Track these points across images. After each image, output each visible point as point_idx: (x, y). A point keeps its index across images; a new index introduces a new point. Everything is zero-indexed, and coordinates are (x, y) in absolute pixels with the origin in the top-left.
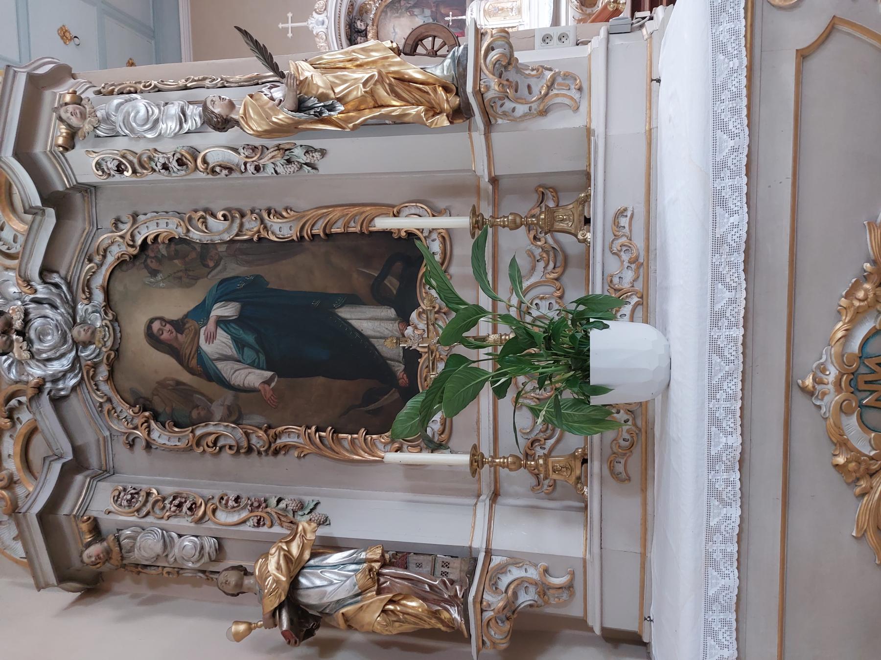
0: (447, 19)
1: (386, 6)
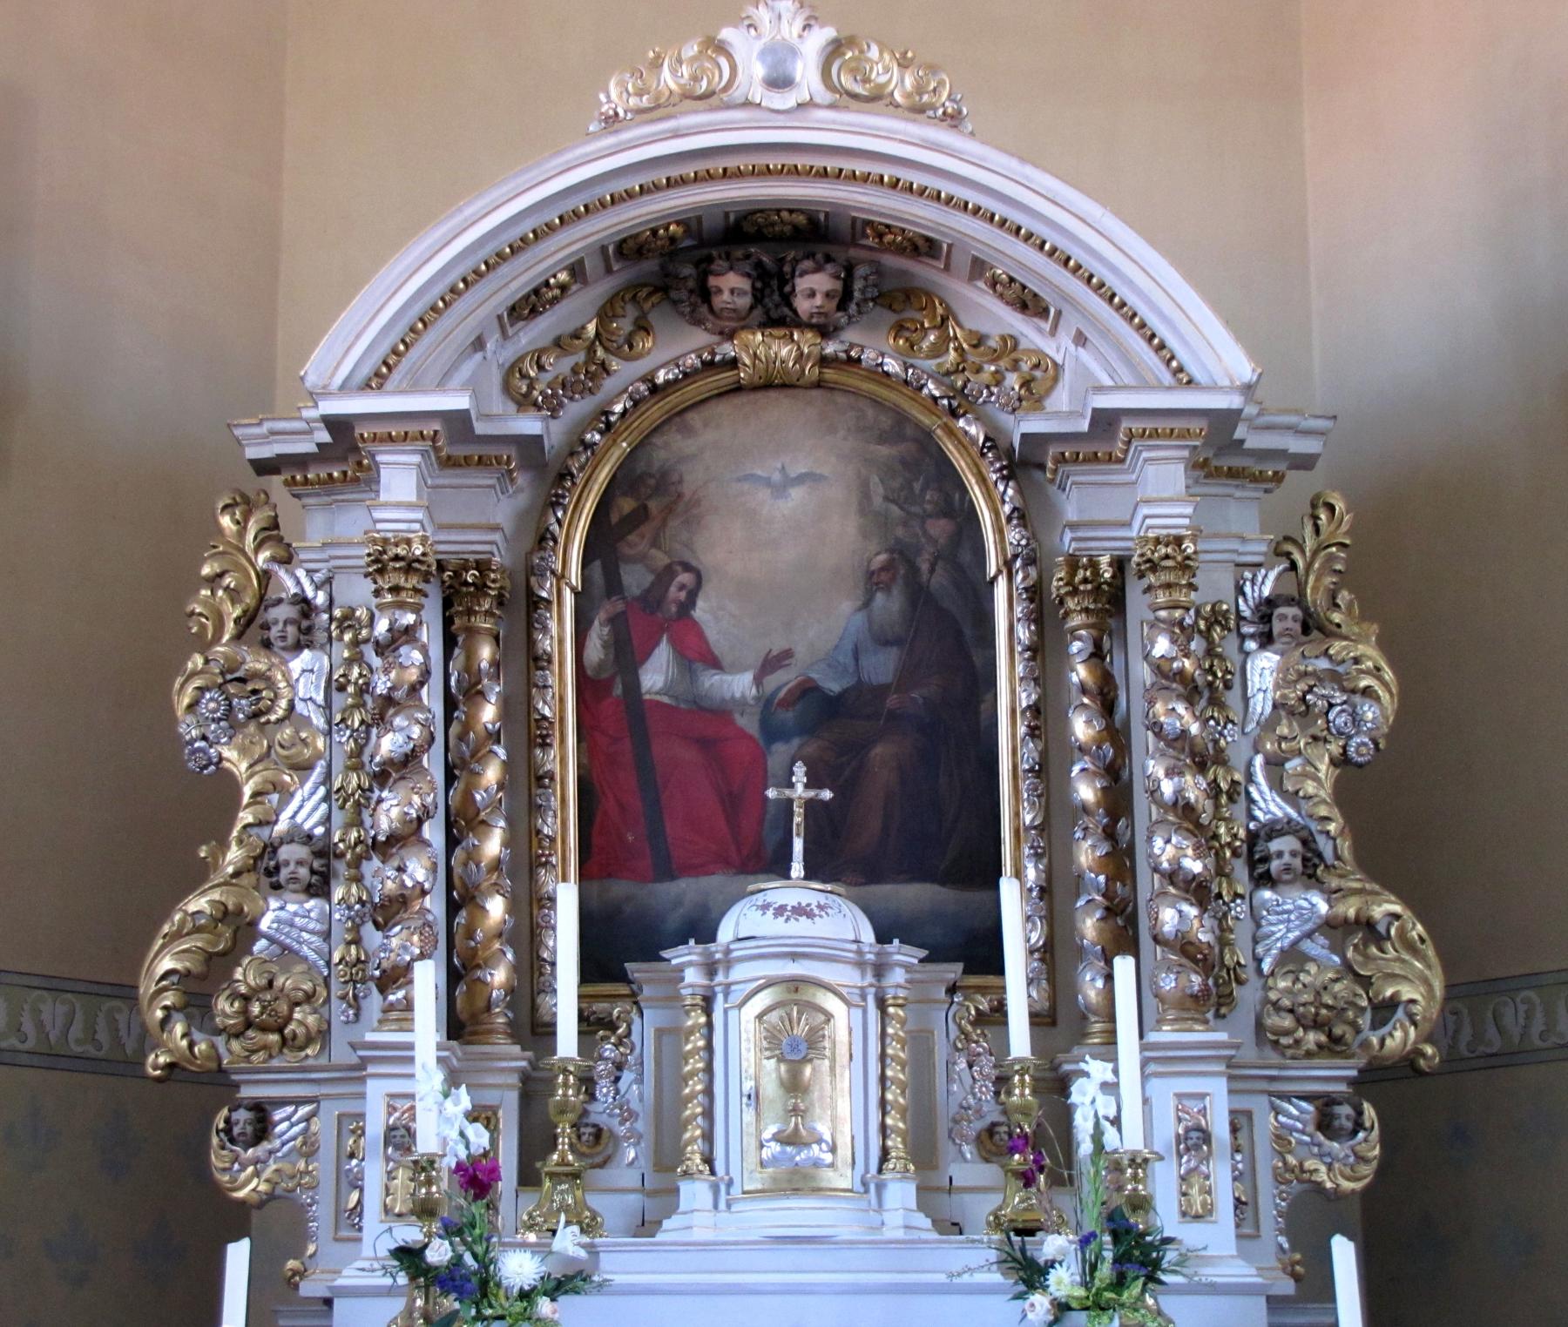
0: (800, 771)
1: (929, 434)
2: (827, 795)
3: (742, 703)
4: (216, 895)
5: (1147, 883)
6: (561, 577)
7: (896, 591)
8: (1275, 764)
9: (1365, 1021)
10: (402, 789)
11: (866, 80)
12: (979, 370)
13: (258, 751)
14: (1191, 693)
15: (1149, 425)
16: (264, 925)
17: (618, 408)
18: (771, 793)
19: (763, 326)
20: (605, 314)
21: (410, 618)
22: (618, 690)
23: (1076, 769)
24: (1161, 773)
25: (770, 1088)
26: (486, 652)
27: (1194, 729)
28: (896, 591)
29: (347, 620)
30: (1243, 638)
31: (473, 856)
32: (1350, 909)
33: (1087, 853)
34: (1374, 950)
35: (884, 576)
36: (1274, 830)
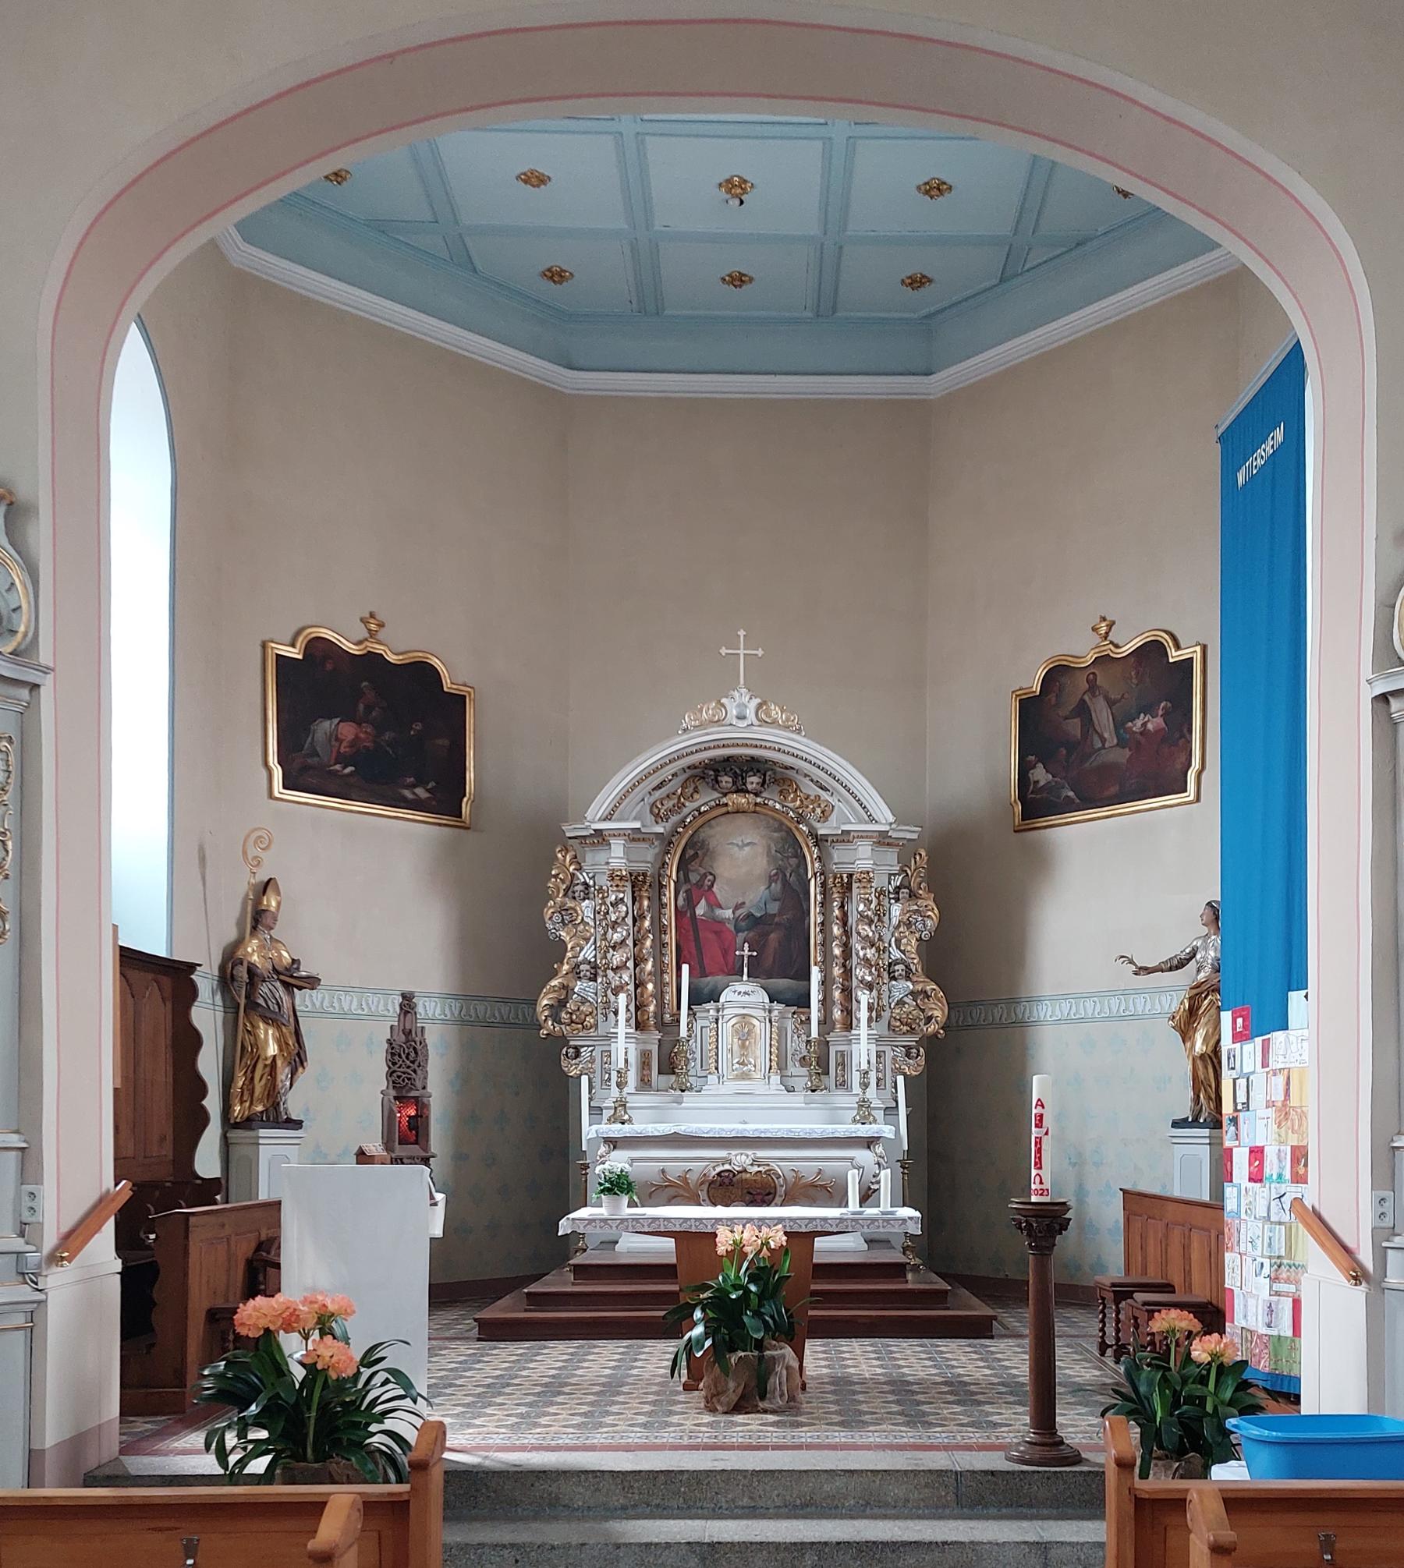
1: (791, 829)
2: (755, 954)
3: (729, 919)
4: (560, 980)
5: (855, 982)
6: (670, 877)
7: (779, 882)
8: (898, 942)
9: (921, 1024)
10: (620, 951)
11: (770, 717)
12: (807, 807)
13: (572, 934)
14: (870, 922)
15: (860, 834)
16: (576, 990)
17: (688, 820)
18: (737, 953)
19: (736, 792)
20: (684, 786)
21: (621, 895)
22: (688, 915)
23: (834, 944)
24: (859, 948)
25: (736, 1048)
26: (646, 903)
27: (871, 934)
28: (779, 882)
29: (600, 890)
30: (890, 899)
31: (642, 970)
32: (919, 987)
33: (837, 971)
34: (926, 1000)
35: (775, 878)
36: (896, 962)
